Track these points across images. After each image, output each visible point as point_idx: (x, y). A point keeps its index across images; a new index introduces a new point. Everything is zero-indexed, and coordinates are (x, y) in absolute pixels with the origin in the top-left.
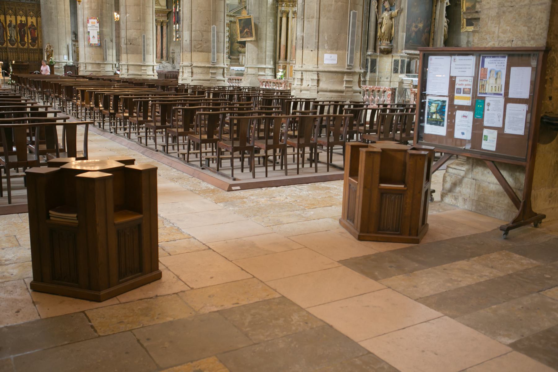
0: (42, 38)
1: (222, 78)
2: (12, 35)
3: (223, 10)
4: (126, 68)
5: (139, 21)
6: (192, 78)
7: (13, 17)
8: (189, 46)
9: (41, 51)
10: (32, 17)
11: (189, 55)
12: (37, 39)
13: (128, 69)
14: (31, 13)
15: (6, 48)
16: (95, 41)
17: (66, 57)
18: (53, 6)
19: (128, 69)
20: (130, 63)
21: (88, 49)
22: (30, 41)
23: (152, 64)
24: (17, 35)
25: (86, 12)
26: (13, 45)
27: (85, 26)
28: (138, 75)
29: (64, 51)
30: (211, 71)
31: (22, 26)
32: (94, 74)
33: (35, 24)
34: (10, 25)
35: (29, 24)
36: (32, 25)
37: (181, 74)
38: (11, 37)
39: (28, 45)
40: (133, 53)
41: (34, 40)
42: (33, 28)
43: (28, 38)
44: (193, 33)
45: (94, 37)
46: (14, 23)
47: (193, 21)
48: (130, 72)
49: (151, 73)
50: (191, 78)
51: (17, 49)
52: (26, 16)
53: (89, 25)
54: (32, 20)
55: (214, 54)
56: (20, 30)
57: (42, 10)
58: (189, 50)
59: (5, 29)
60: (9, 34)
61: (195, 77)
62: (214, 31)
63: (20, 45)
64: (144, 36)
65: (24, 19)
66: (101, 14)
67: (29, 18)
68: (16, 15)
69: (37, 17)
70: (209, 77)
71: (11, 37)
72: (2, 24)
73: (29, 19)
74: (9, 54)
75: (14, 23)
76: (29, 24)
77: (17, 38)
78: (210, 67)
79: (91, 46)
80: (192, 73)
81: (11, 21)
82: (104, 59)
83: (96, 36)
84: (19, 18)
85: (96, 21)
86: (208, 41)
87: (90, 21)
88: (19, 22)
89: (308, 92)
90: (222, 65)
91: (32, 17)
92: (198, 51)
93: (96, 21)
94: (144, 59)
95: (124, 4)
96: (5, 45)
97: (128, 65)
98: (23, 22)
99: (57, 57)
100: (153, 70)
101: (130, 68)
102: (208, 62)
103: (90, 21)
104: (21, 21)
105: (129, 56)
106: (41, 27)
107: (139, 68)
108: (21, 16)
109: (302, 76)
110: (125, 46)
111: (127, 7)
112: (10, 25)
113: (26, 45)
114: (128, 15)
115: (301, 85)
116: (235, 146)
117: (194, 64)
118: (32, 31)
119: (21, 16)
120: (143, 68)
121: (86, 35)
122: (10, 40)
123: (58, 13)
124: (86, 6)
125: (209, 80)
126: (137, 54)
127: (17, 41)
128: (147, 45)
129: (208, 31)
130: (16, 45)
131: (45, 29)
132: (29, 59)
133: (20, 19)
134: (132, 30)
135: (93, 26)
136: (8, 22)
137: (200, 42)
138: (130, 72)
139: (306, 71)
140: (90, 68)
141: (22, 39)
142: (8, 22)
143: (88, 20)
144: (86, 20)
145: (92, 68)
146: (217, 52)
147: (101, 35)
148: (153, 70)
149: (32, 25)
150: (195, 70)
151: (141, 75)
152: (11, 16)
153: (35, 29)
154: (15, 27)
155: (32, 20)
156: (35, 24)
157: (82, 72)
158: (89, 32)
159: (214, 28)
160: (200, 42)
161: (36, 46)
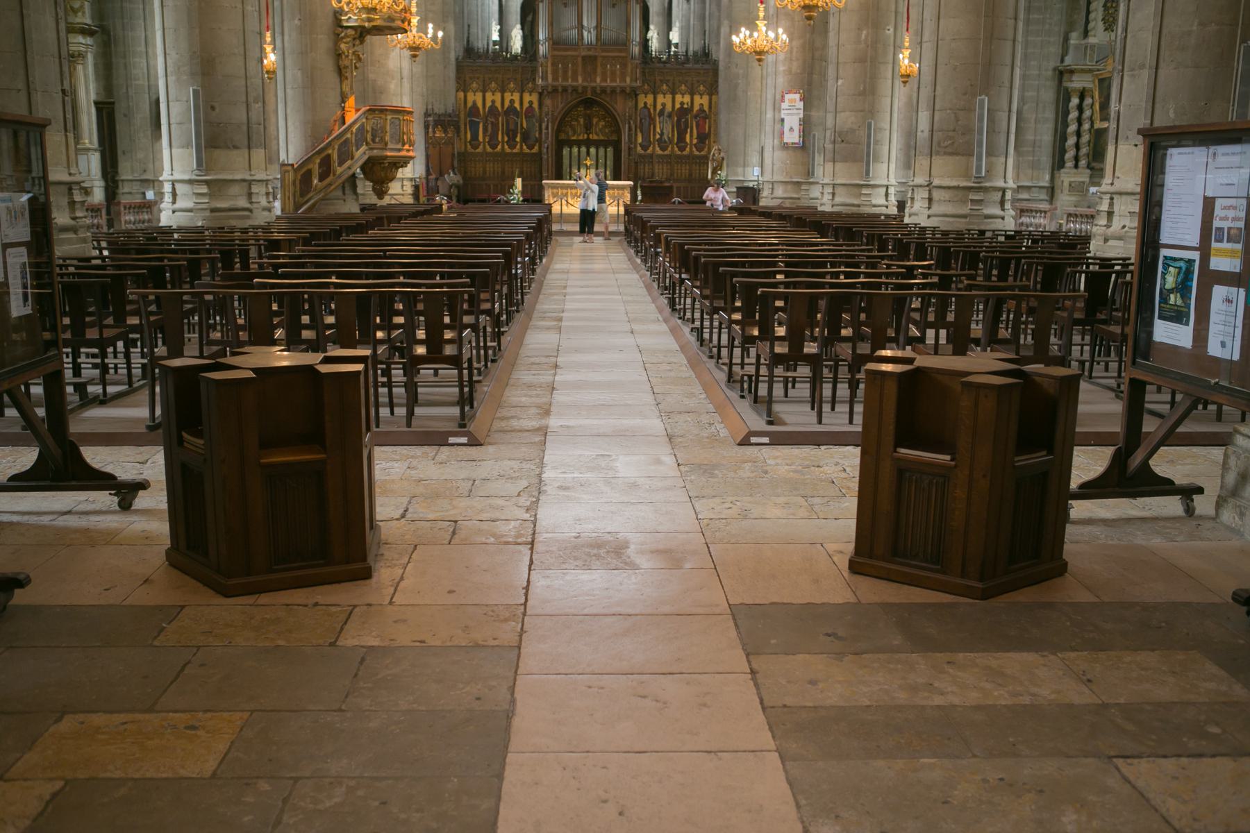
0: (716, 134)
1: (998, 212)
3: (1008, 61)
4: (830, 190)
5: (863, 94)
6: (931, 212)
7: (669, 96)
8: (928, 144)
9: (704, 160)
11: (926, 162)
12: (708, 136)
13: (833, 194)
14: (702, 88)
15: (651, 156)
16: (793, 137)
17: (757, 171)
19: (833, 194)
20: (839, 181)
21: (779, 154)
22: (695, 141)
23: (885, 183)
25: (781, 81)
26: (663, 149)
27: (776, 109)
28: (853, 205)
29: (755, 159)
30: (973, 196)
31: (683, 112)
32: (787, 204)
33: (706, 108)
34: (662, 113)
35: (696, 108)
36: (702, 110)
37: (909, 204)
38: (662, 134)
40: (845, 160)
41: (703, 138)
42: (703, 116)
43: (691, 136)
44: (937, 114)
45: (791, 129)
46: (669, 108)
47: (938, 87)
48: (838, 200)
49: (883, 201)
50: (927, 212)
51: (669, 156)
52: (692, 95)
53: (785, 105)
54: (701, 101)
55: (979, 159)
56: (679, 121)
57: (720, 80)
58: (927, 151)
59: (652, 120)
60: (658, 130)
61: (936, 209)
62: (982, 108)
64: (870, 125)
65: (687, 99)
66: (810, 84)
67: (697, 98)
68: (673, 93)
69: (711, 95)
70: (965, 210)
71: (662, 134)
73: (697, 98)
75: (669, 108)
76: (696, 108)
78: (970, 188)
79: (785, 147)
80: (930, 200)
81: (664, 105)
82: (810, 173)
83: (797, 128)
84: (679, 98)
85: (797, 96)
86: (968, 131)
87: (787, 97)
88: (678, 106)
89: (1120, 243)
90: (1001, 184)
92: (945, 153)
93: (797, 96)
94: (868, 173)
95: (834, 61)
96: (650, 151)
97: (834, 185)
99: (740, 170)
100: (887, 195)
101: (839, 190)
102: (967, 176)
103: (787, 97)
104: (682, 103)
105: (839, 166)
106: (717, 114)
107: (856, 190)
108: (683, 95)
109: (1111, 204)
110: (831, 146)
111: (841, 66)
114: (840, 82)
115: (1108, 226)
116: (859, 351)
117: (936, 182)
119: (683, 95)
120: (864, 191)
121: (778, 126)
122: (660, 141)
124: (781, 68)
125: (965, 216)
126: (855, 161)
127: (671, 141)
128: (876, 142)
129: (969, 109)
131: (723, 117)
132: (690, 175)
134: (848, 113)
135: (792, 107)
136: (659, 107)
137: (951, 134)
138: (838, 200)
139: (1120, 194)
140: (780, 192)
141: (681, 139)
142: (659, 107)
143: (783, 97)
144: (778, 97)
145: (785, 191)
146: (988, 154)
147: (806, 124)
148: (887, 195)
149: (702, 110)
150: (936, 195)
151: (859, 206)
154: (670, 116)
155: (701, 101)
156: (706, 108)
157: (765, 201)
158: (783, 120)
159: (983, 100)
160: (951, 134)
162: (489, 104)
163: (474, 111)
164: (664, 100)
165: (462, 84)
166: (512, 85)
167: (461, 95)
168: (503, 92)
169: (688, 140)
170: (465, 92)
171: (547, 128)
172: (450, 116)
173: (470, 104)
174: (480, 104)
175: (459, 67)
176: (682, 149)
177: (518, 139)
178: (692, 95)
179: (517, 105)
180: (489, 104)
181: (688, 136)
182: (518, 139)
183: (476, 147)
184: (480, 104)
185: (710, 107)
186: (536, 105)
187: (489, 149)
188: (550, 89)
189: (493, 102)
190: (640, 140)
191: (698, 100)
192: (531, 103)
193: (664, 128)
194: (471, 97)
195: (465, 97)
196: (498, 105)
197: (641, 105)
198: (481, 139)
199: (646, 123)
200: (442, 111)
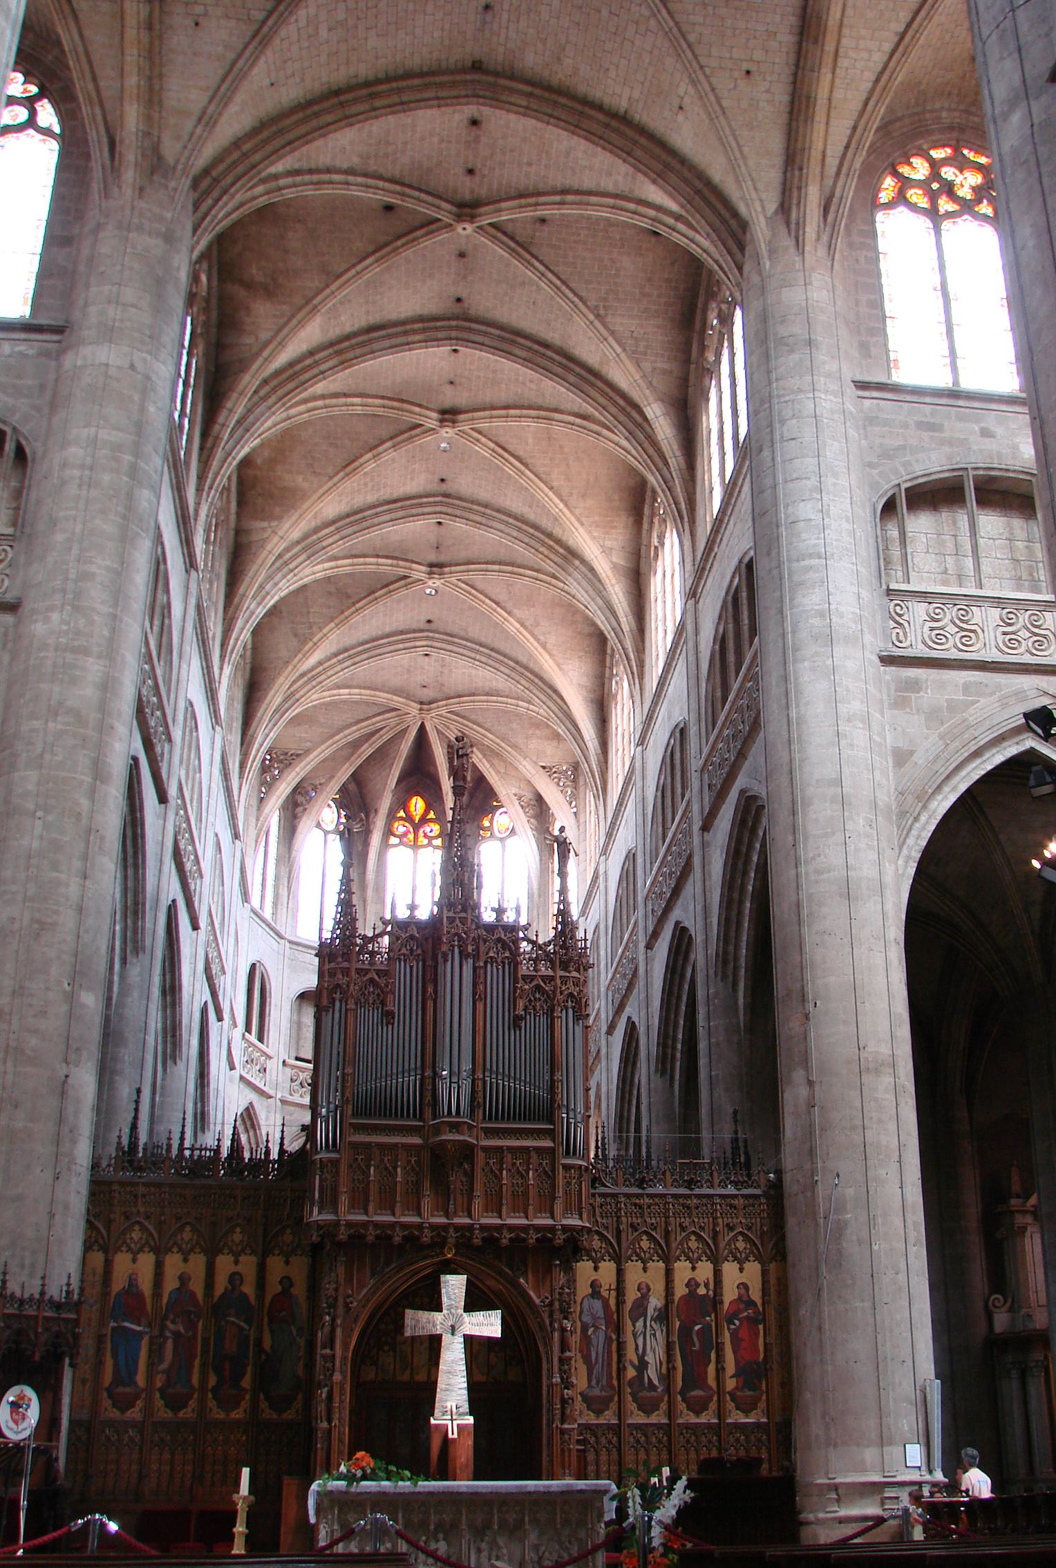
18: (850, 1192)
31: (702, 1305)
75: (655, 1302)
112: (640, 1308)
123: (870, 1222)
133: (688, 1274)
162: (171, 1284)
163: (130, 1303)
164: (646, 1277)
165: (102, 1232)
166: (237, 1236)
167: (98, 1258)
168: (212, 1254)
170: (108, 1251)
171: (331, 1343)
172: (58, 1306)
173: (118, 1284)
174: (146, 1286)
175: (100, 1190)
177: (246, 1382)
179: (248, 1289)
180: (171, 1284)
181: (711, 1369)
182: (246, 1382)
183: (123, 1404)
184: (146, 1286)
186: (299, 1291)
187: (163, 1413)
188: (343, 1235)
189: (183, 1279)
190: (580, 1380)
192: (287, 1282)
193: (650, 1346)
194: (122, 1262)
195: (108, 1264)
196: (197, 1287)
198: (141, 1380)
200: (34, 1289)
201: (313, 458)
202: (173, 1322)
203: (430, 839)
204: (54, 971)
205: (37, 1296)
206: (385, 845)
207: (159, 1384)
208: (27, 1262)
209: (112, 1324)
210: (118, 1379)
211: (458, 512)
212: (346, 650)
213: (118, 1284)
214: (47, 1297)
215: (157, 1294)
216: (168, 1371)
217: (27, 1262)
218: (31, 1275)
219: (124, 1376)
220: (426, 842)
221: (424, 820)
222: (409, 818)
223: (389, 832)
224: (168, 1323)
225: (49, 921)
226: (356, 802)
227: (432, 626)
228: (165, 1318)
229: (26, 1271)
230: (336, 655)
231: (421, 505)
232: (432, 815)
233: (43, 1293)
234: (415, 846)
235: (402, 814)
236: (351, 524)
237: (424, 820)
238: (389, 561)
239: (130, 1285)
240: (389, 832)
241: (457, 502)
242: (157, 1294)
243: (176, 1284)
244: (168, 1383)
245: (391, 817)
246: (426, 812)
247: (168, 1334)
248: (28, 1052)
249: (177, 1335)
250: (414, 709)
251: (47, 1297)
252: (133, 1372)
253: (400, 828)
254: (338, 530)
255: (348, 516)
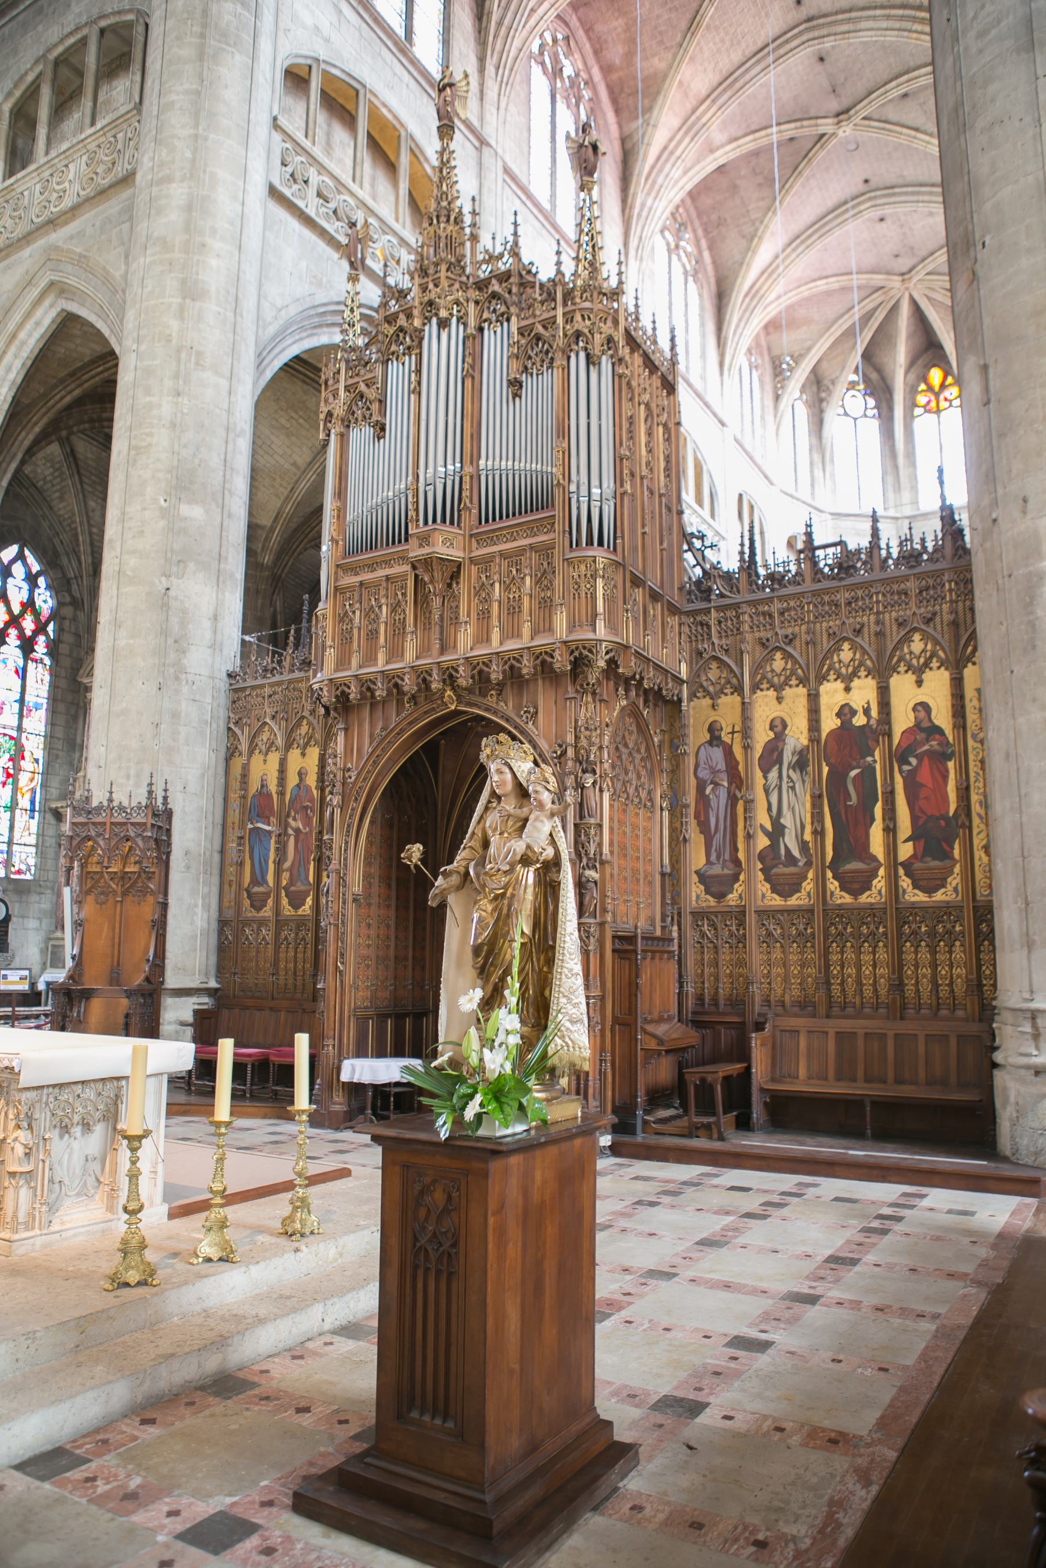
2: (787, 820)
7: (797, 696)
10: (919, 672)
24: (817, 817)
26: (785, 887)
33: (942, 718)
34: (772, 755)
35: (902, 720)
36: (925, 727)
39: (893, 881)
42: (937, 752)
43: (890, 830)
46: (798, 736)
52: (882, 674)
54: (920, 694)
56: (837, 778)
59: (737, 779)
60: (763, 818)
63: (833, 885)
65: (864, 692)
67: (902, 685)
71: (777, 832)
72: (728, 751)
74: (756, 956)
75: (798, 736)
76: (902, 720)
77: (819, 833)
81: (779, 727)
84: (832, 695)
88: (829, 723)
91: (919, 672)
98: (859, 720)
104: (845, 712)
113: (879, 883)
118: (925, 776)
122: (769, 858)
130: (808, 886)
132: (898, 986)
136: (762, 736)
141: (851, 842)
149: (925, 727)
152: (778, 688)
153: (941, 757)
154: (801, 764)
155: (920, 694)
156: (942, 718)
161: (954, 880)
162: (292, 780)
169: (877, 844)
173: (254, 787)
176: (857, 884)
178: (882, 674)
180: (292, 780)
185: (959, 711)
191: (904, 690)
197: (696, 736)
198: (270, 878)
199: (719, 799)
201: (660, 33)
202: (295, 819)
203: (951, 401)
204: (149, 490)
205: (105, 804)
206: (909, 418)
207: (284, 883)
208: (132, 772)
209: (250, 826)
210: (254, 882)
211: (824, 31)
212: (798, 237)
213: (254, 787)
214: (115, 804)
215: (281, 794)
216: (291, 870)
217: (132, 772)
218: (137, 785)
219: (258, 879)
220: (947, 404)
221: (943, 386)
222: (930, 388)
223: (911, 404)
224: (290, 820)
225: (144, 444)
226: (879, 389)
227: (873, 184)
228: (288, 815)
229: (131, 782)
230: (789, 245)
231: (787, 42)
232: (950, 380)
233: (110, 800)
234: (938, 411)
235: (923, 387)
236: (725, 90)
237: (943, 386)
238: (793, 125)
239: (262, 786)
240: (911, 404)
241: (821, 21)
242: (281, 794)
243: (296, 781)
244: (291, 882)
245: (912, 392)
246: (945, 378)
247: (290, 831)
248: (129, 573)
249: (297, 831)
250: (895, 282)
251: (115, 804)
252: (264, 873)
253: (922, 399)
254: (714, 101)
255: (720, 84)
